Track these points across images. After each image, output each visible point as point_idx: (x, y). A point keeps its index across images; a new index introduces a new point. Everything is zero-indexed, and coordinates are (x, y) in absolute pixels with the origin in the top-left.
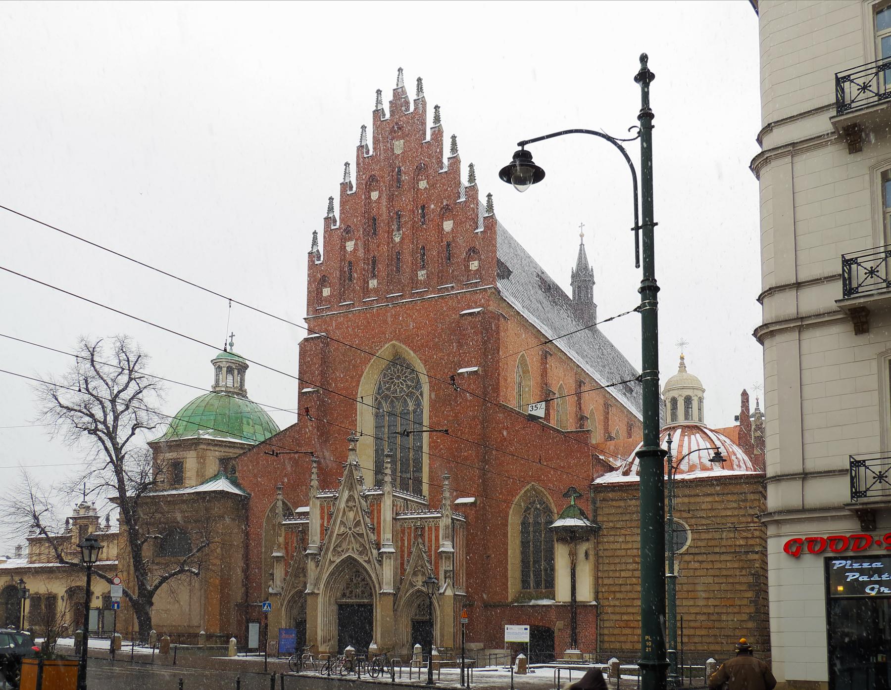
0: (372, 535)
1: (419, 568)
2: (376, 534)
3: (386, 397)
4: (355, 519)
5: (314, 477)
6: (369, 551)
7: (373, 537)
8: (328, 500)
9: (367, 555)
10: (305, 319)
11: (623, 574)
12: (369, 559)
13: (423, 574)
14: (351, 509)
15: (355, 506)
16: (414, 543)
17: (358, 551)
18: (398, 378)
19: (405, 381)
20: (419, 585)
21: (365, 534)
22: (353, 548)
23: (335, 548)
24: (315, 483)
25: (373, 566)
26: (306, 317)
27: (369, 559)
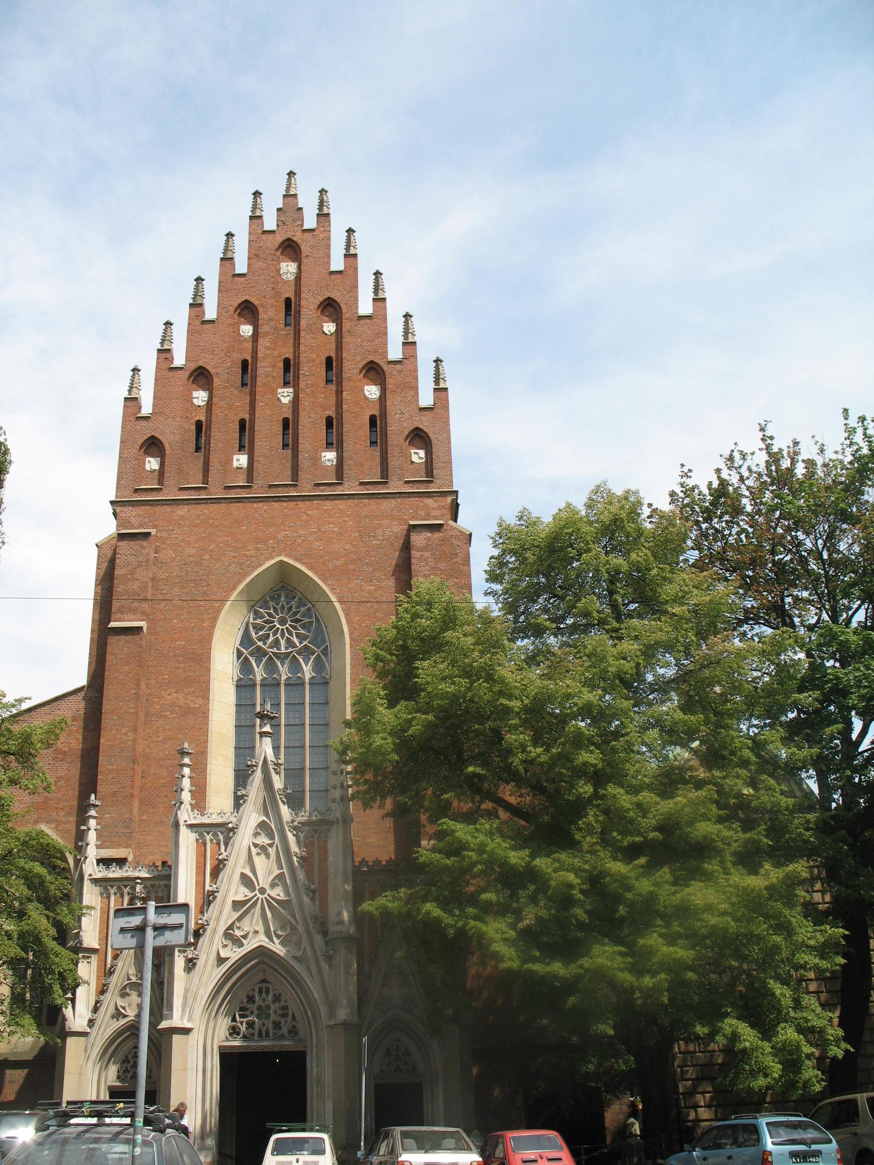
2: (317, 902)
3: (259, 653)
4: (270, 872)
5: (186, 783)
10: (112, 503)
12: (304, 951)
15: (271, 845)
18: (283, 622)
19: (295, 628)
24: (186, 796)
25: (314, 969)
26: (113, 499)
27: (304, 951)
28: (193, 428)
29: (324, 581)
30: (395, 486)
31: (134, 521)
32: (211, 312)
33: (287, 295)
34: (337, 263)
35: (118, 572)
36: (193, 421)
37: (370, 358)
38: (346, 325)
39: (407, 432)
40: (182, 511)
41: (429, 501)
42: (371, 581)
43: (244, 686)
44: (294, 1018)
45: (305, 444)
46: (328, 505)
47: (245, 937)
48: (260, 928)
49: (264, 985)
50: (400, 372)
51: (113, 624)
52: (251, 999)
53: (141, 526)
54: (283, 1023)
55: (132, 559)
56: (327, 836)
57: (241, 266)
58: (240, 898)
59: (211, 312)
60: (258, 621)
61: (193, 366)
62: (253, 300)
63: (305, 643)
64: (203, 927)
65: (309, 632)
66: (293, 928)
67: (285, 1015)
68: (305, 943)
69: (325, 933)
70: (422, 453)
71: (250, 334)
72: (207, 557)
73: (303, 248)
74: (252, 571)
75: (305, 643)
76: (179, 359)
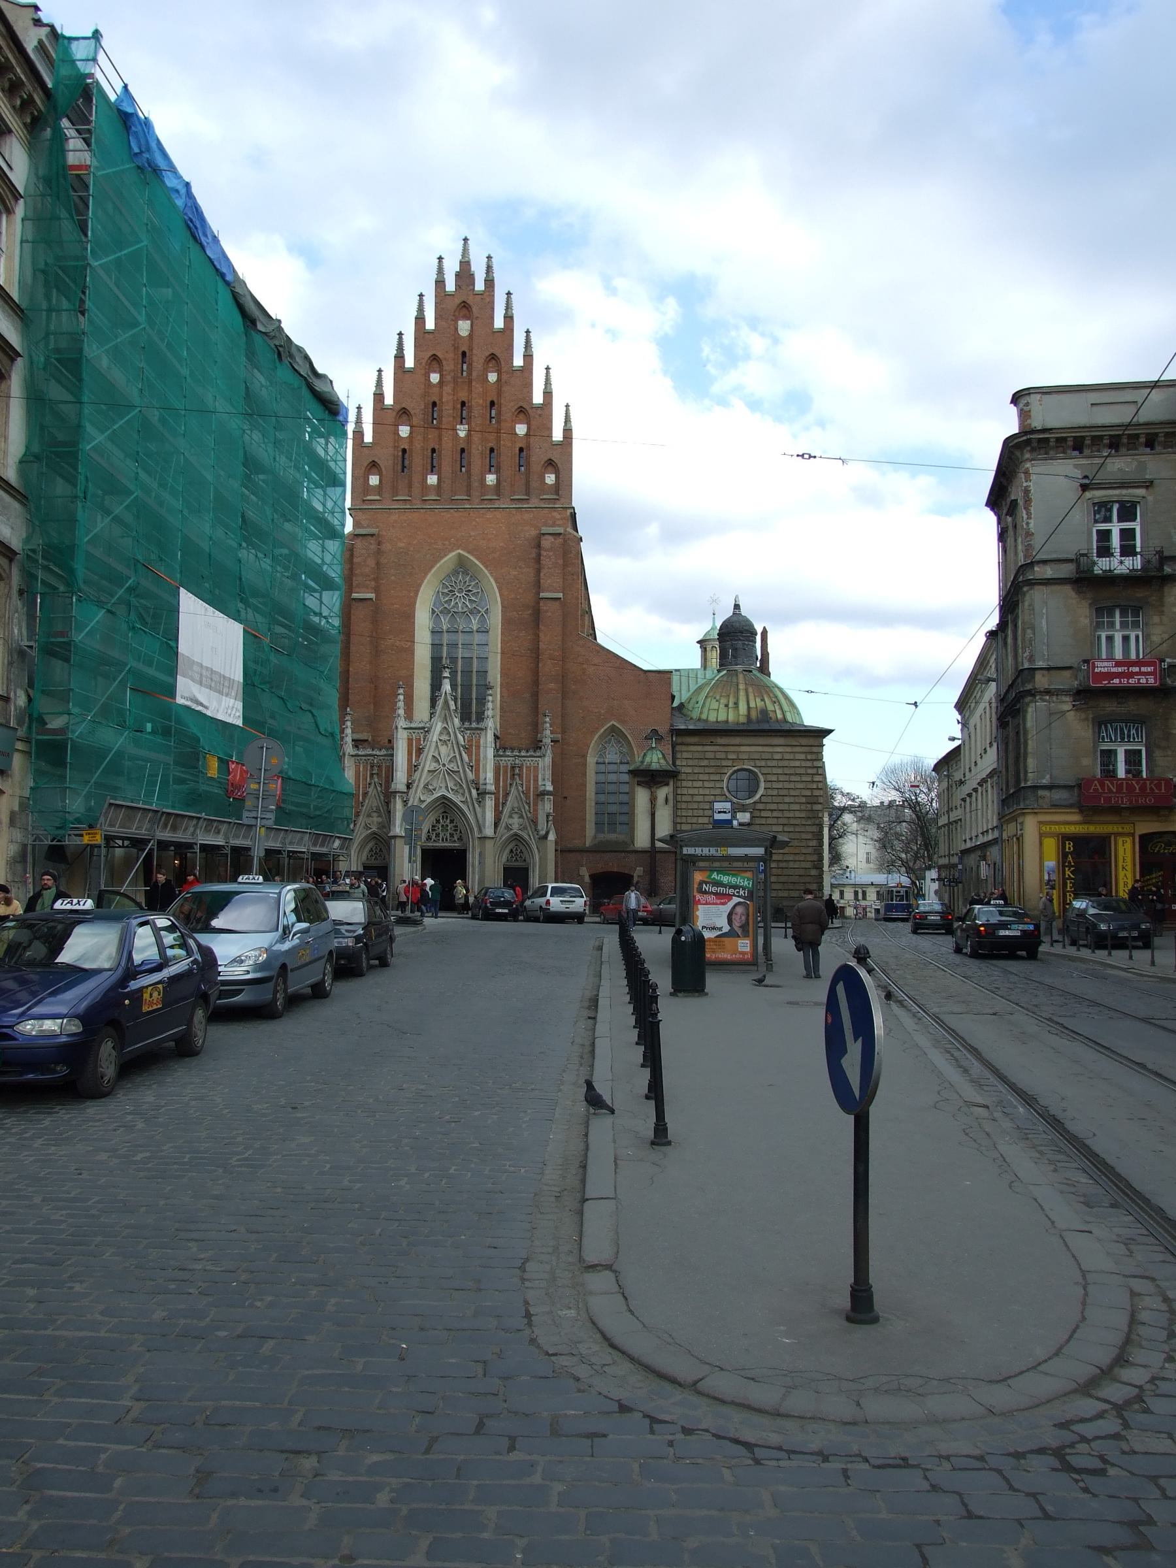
0: (470, 773)
1: (516, 810)
3: (446, 611)
4: (449, 756)
5: (401, 704)
6: (466, 791)
7: (471, 776)
8: (417, 731)
9: (463, 795)
11: (701, 820)
13: (521, 817)
14: (445, 742)
15: (449, 740)
16: (511, 784)
17: (452, 790)
18: (460, 591)
20: (515, 828)
21: (461, 771)
22: (447, 787)
23: (427, 784)
24: (401, 712)
25: (471, 808)
28: (400, 454)
29: (486, 567)
30: (534, 502)
31: (365, 523)
32: (410, 362)
33: (463, 349)
34: (499, 323)
35: (355, 560)
36: (399, 449)
37: (521, 404)
38: (504, 377)
39: (542, 463)
40: (395, 517)
41: (555, 514)
42: (516, 568)
44: (461, 832)
45: (476, 469)
46: (489, 515)
47: (434, 790)
48: (443, 785)
49: (445, 814)
50: (540, 415)
51: (355, 595)
52: (438, 821)
53: (368, 526)
54: (455, 836)
55: (364, 551)
56: (480, 737)
57: (430, 324)
58: (432, 768)
59: (410, 362)
60: (446, 591)
61: (398, 407)
62: (439, 354)
63: (474, 605)
64: (411, 783)
65: (476, 598)
66: (461, 785)
67: (456, 830)
68: (467, 794)
69: (478, 789)
70: (553, 477)
71: (437, 381)
72: (412, 549)
73: (474, 310)
74: (441, 560)
75: (474, 605)
76: (389, 400)
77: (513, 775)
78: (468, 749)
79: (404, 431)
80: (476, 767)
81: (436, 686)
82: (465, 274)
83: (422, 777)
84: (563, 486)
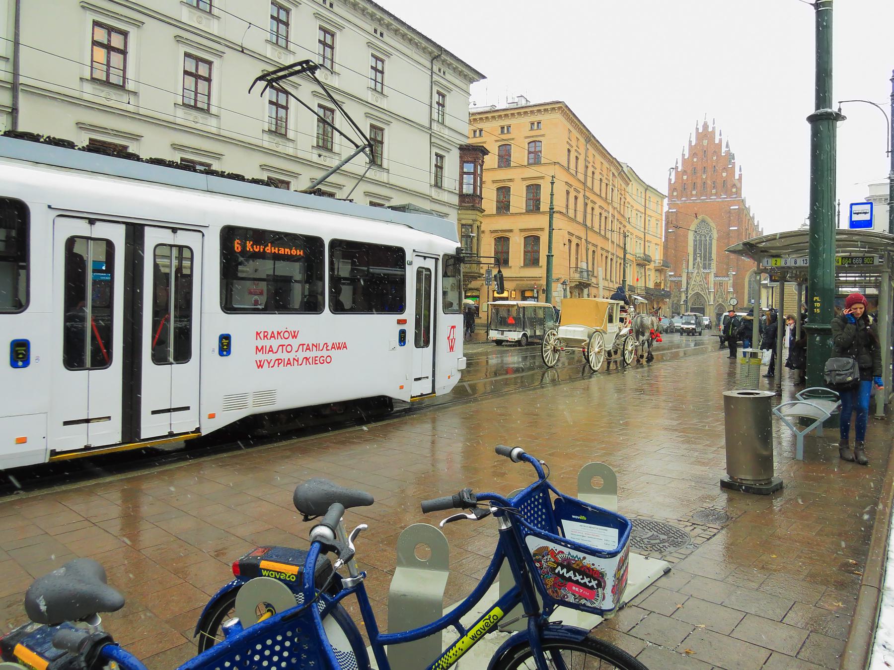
14: (698, 276)
43: (695, 241)
77: (720, 286)
78: (705, 278)
79: (685, 177)
80: (707, 284)
81: (695, 259)
82: (705, 126)
83: (691, 287)
84: (738, 193)
